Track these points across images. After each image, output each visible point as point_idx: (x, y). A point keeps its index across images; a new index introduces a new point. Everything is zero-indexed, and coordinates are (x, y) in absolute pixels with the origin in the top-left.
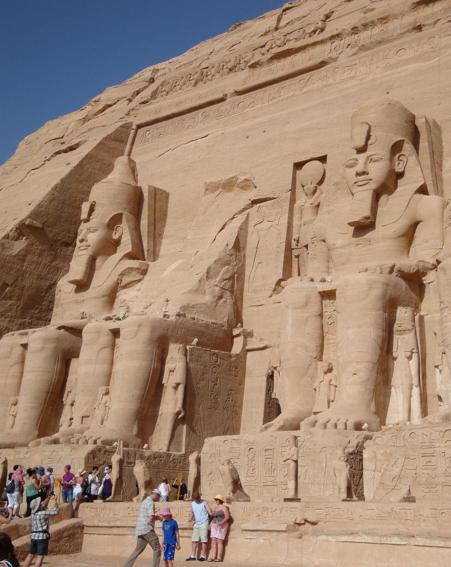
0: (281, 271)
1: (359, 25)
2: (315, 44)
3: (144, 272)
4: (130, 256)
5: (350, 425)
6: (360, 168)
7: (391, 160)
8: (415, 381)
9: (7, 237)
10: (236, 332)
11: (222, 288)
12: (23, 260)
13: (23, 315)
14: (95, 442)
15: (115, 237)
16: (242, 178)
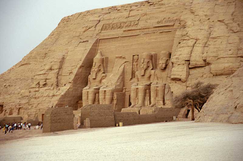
0: (131, 77)
6: (142, 66)
9: (78, 69)
16: (123, 56)
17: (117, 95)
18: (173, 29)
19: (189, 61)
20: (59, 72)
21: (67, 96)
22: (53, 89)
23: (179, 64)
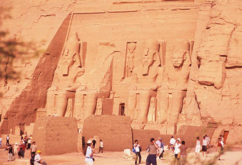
3: (84, 72)
5: (142, 123)
7: (153, 58)
8: (154, 113)
10: (111, 92)
11: (108, 81)
12: (44, 64)
15: (74, 60)
17: (103, 102)
18: (193, 6)
19: (226, 56)
21: (23, 99)
23: (210, 60)
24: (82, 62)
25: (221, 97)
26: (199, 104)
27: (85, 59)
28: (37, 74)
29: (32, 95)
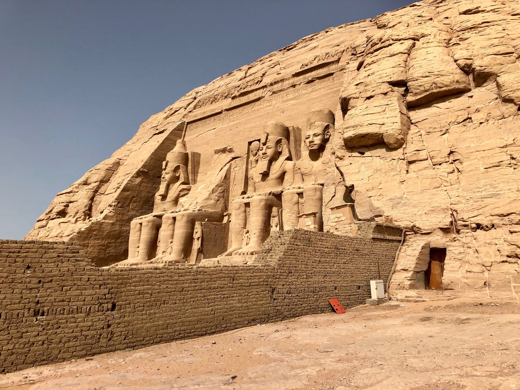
1: (273, 82)
2: (256, 90)
3: (189, 190)
4: (183, 183)
6: (263, 151)
7: (276, 147)
12: (141, 186)
13: (142, 208)
14: (166, 262)
15: (177, 175)
16: (229, 148)
20: (99, 187)
21: (96, 235)
22: (76, 221)
23: (368, 95)
24: (190, 178)
25: (405, 167)
26: (351, 191)
27: (197, 176)
28: (126, 198)
29: (117, 228)
